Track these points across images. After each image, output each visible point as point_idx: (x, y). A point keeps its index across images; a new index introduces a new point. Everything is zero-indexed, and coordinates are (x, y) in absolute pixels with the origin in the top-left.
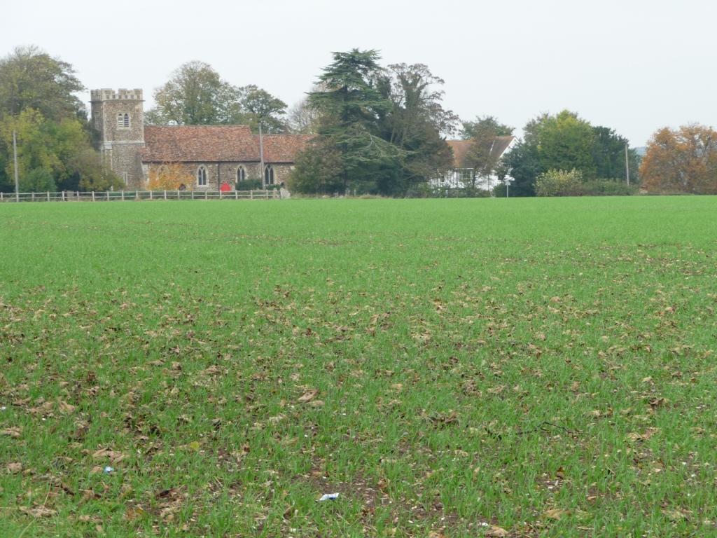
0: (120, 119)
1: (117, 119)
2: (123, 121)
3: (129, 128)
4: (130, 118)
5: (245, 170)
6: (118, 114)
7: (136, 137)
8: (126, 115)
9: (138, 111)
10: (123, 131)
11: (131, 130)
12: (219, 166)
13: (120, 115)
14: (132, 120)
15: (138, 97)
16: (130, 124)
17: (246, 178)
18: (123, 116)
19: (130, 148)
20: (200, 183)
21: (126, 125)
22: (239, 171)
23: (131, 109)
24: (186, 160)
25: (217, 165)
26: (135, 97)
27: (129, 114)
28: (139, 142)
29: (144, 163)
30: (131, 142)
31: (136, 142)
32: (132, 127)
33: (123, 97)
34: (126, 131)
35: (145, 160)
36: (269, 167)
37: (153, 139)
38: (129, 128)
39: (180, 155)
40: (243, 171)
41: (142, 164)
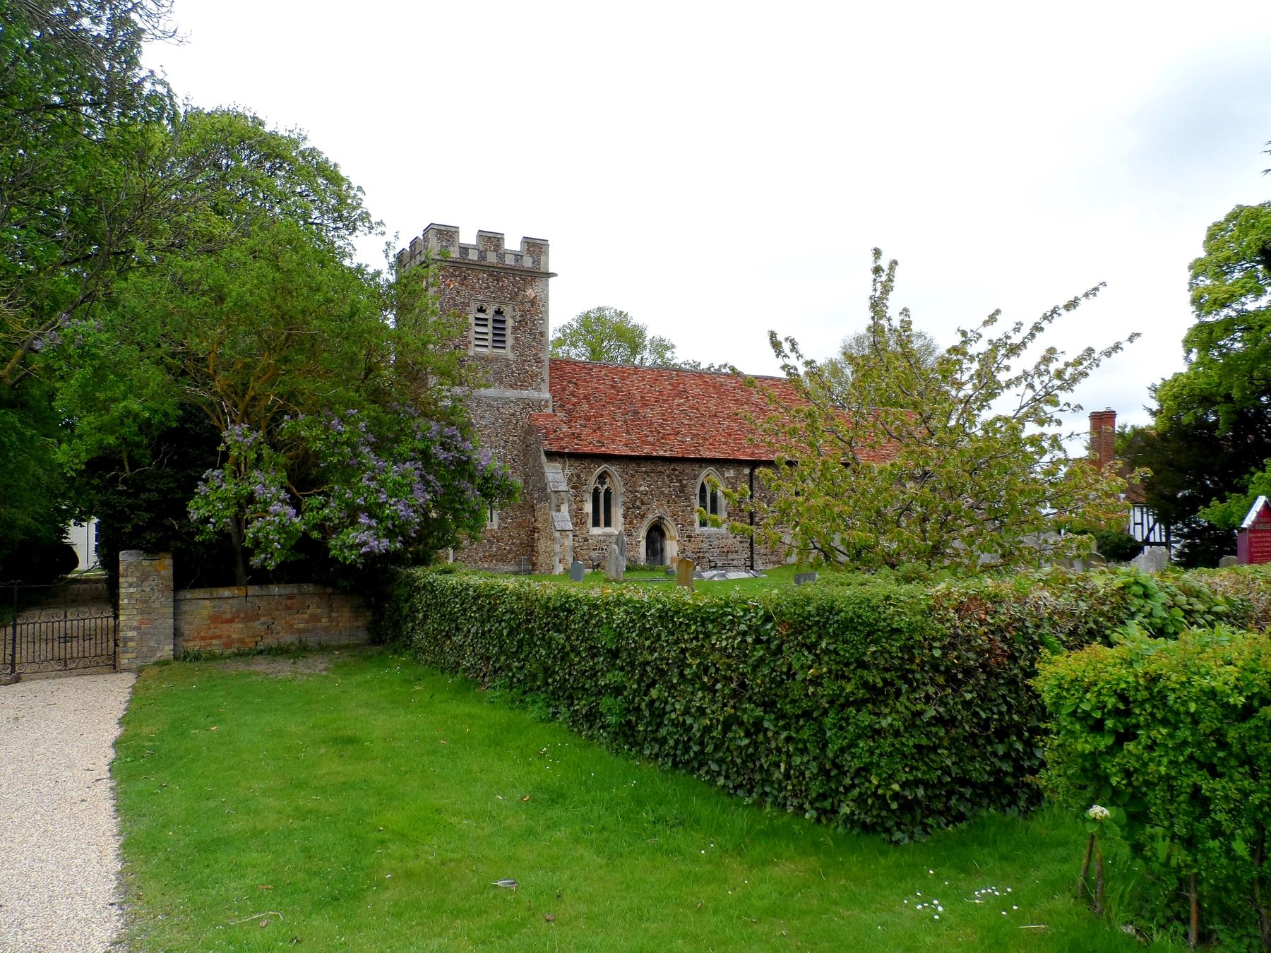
0: (481, 322)
1: (471, 319)
2: (489, 330)
3: (508, 353)
4: (510, 323)
6: (474, 307)
7: (523, 379)
8: (499, 312)
9: (533, 302)
10: (486, 360)
11: (511, 356)
12: (751, 474)
13: (481, 310)
14: (515, 329)
15: (536, 262)
16: (510, 340)
18: (490, 315)
19: (507, 412)
21: (499, 340)
24: (667, 454)
25: (747, 471)
26: (528, 262)
27: (508, 311)
28: (535, 394)
29: (551, 455)
30: (510, 393)
32: (513, 348)
33: (492, 258)
35: (554, 448)
37: (572, 394)
38: (508, 353)
39: (650, 439)
41: (544, 458)
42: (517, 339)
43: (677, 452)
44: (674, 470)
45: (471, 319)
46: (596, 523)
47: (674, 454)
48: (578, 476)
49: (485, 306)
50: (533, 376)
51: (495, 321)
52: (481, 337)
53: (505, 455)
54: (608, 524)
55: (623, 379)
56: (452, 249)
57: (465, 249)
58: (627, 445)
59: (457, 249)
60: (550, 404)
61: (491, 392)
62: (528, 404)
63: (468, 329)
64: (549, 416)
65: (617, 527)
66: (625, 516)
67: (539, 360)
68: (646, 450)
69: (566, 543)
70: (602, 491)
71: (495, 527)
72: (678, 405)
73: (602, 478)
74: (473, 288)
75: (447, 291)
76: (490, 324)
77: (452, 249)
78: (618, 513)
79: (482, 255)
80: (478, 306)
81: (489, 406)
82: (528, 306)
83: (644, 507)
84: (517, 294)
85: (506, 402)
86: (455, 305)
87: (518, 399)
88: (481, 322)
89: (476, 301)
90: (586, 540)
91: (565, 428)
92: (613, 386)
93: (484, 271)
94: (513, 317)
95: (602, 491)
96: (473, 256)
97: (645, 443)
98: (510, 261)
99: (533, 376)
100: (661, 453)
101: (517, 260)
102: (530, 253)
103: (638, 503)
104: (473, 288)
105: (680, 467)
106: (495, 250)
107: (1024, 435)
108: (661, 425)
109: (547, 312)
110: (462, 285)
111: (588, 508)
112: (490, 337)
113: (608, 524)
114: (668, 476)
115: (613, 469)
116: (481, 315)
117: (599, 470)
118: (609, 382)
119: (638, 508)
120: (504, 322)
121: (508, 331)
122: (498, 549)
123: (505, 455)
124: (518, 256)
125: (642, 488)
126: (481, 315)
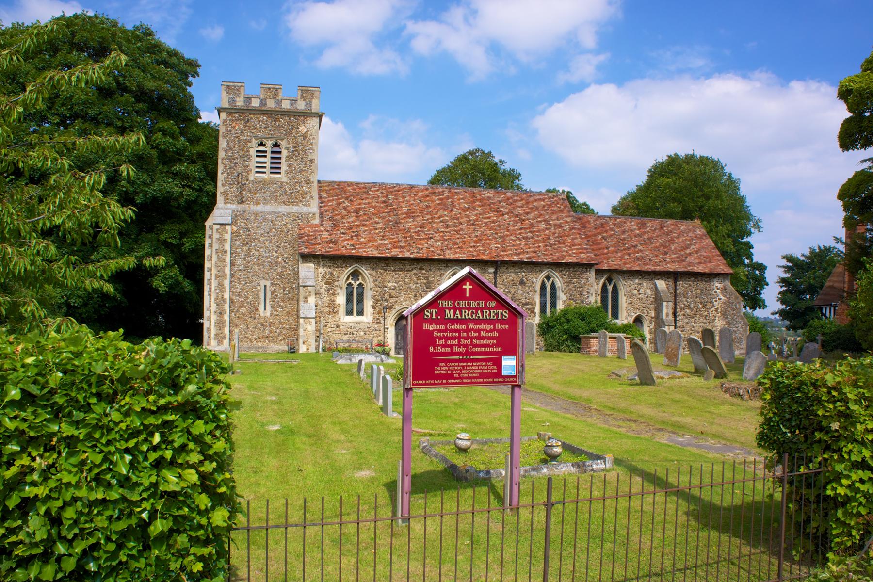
1: (253, 152)
2: (268, 160)
4: (285, 153)
5: (559, 284)
6: (254, 142)
7: (298, 198)
8: (276, 145)
9: (305, 136)
10: (264, 183)
14: (289, 158)
16: (284, 167)
17: (560, 306)
18: (269, 147)
19: (279, 223)
21: (276, 167)
22: (543, 287)
23: (288, 134)
25: (492, 270)
26: (301, 106)
27: (283, 143)
30: (283, 209)
31: (295, 209)
32: (287, 173)
33: (271, 104)
34: (272, 183)
36: (609, 280)
37: (345, 209)
38: (282, 177)
40: (553, 287)
42: (290, 166)
43: (423, 254)
45: (253, 152)
46: (349, 312)
47: (419, 255)
48: (331, 274)
49: (265, 141)
50: (303, 195)
51: (272, 152)
52: (260, 166)
53: (278, 257)
54: (360, 313)
55: (396, 196)
56: (238, 99)
58: (377, 248)
59: (242, 99)
60: (317, 216)
61: (268, 208)
62: (297, 217)
63: (249, 160)
64: (316, 225)
65: (368, 317)
66: (374, 308)
67: (308, 182)
68: (395, 252)
69: (309, 328)
71: (268, 314)
72: (441, 216)
73: (355, 274)
74: (255, 128)
76: (269, 155)
77: (238, 99)
78: (368, 304)
79: (263, 102)
80: (259, 141)
81: (265, 219)
82: (300, 140)
83: (391, 300)
84: (291, 130)
85: (279, 215)
87: (289, 213)
88: (261, 154)
89: (256, 138)
90: (338, 326)
91: (325, 235)
92: (384, 202)
93: (264, 115)
94: (287, 149)
96: (255, 103)
97: (395, 246)
98: (286, 105)
99: (303, 195)
100: (407, 255)
101: (292, 104)
102: (304, 98)
103: (386, 296)
106: (274, 98)
107: (130, 213)
108: (417, 233)
109: (317, 144)
110: (245, 126)
111: (341, 299)
112: (268, 165)
113: (360, 313)
116: (262, 148)
118: (382, 199)
119: (387, 300)
120: (280, 153)
121: (283, 160)
122: (271, 332)
123: (278, 257)
125: (391, 284)
126: (262, 148)
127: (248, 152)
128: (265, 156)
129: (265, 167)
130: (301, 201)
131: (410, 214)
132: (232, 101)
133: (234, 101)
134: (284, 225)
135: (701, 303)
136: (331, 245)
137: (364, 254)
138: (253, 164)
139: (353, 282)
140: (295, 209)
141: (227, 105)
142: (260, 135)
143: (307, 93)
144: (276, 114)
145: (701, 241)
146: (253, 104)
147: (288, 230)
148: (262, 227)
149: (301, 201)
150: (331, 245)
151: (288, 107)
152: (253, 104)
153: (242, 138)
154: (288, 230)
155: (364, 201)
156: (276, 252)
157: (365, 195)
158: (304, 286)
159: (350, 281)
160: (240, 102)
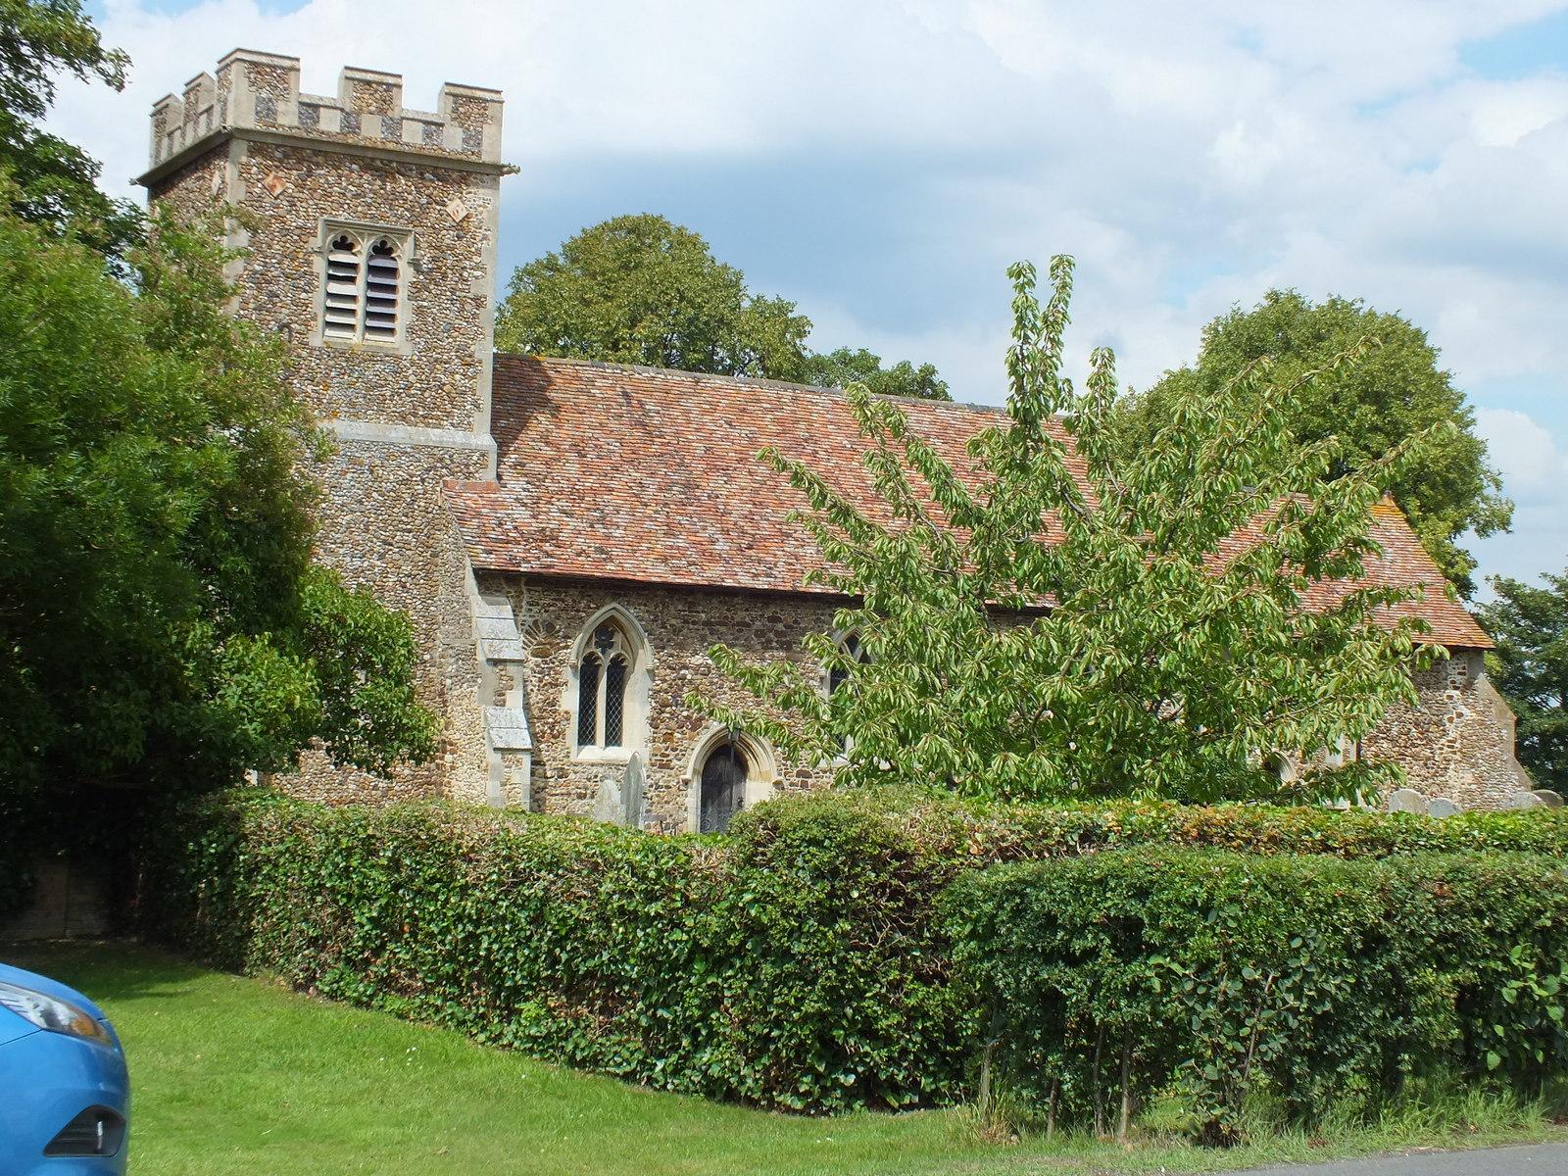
0: (343, 273)
2: (358, 289)
3: (398, 343)
4: (406, 276)
9: (461, 228)
10: (349, 357)
13: (343, 245)
14: (417, 290)
15: (474, 139)
16: (404, 313)
18: (360, 256)
19: (390, 477)
20: (586, 736)
21: (380, 317)
23: (416, 219)
24: (762, 584)
26: (452, 141)
27: (404, 252)
29: (490, 580)
30: (401, 434)
31: (434, 435)
33: (372, 131)
34: (372, 357)
35: (492, 561)
38: (398, 343)
39: (722, 546)
41: (471, 582)
42: (420, 312)
44: (774, 619)
45: (319, 266)
51: (372, 270)
52: (339, 306)
53: (384, 573)
54: (614, 737)
55: (666, 405)
56: (281, 106)
57: (311, 108)
58: (665, 560)
59: (293, 107)
60: (493, 458)
64: (488, 488)
66: (654, 723)
70: (605, 662)
73: (605, 633)
74: (327, 195)
75: (268, 200)
76: (362, 276)
78: (636, 710)
81: (353, 461)
82: (449, 237)
85: (392, 453)
86: (285, 232)
91: (522, 515)
94: (415, 264)
95: (605, 662)
96: (330, 124)
97: (713, 558)
98: (412, 137)
100: (746, 581)
101: (428, 135)
102: (459, 118)
104: (327, 195)
105: (788, 615)
106: (381, 111)
108: (749, 517)
110: (301, 187)
111: (570, 700)
114: (760, 634)
115: (630, 614)
117: (598, 616)
121: (401, 296)
123: (384, 573)
124: (432, 126)
127: (309, 263)
128: (352, 280)
129: (352, 312)
130: (449, 415)
131: (715, 464)
132: (266, 110)
133: (271, 112)
134: (404, 482)
135: (1417, 725)
136: (547, 547)
137: (640, 576)
138: (318, 301)
139: (598, 651)
140: (434, 435)
141: (249, 122)
142: (343, 217)
143: (470, 104)
144: (384, 163)
145: (1405, 560)
146: (323, 126)
147: (414, 498)
148: (346, 482)
149: (449, 415)
150: (547, 547)
151: (419, 140)
152: (323, 126)
153: (293, 222)
154: (414, 498)
155: (587, 419)
156: (381, 557)
157: (583, 399)
158: (496, 662)
159: (593, 649)
160: (288, 118)
